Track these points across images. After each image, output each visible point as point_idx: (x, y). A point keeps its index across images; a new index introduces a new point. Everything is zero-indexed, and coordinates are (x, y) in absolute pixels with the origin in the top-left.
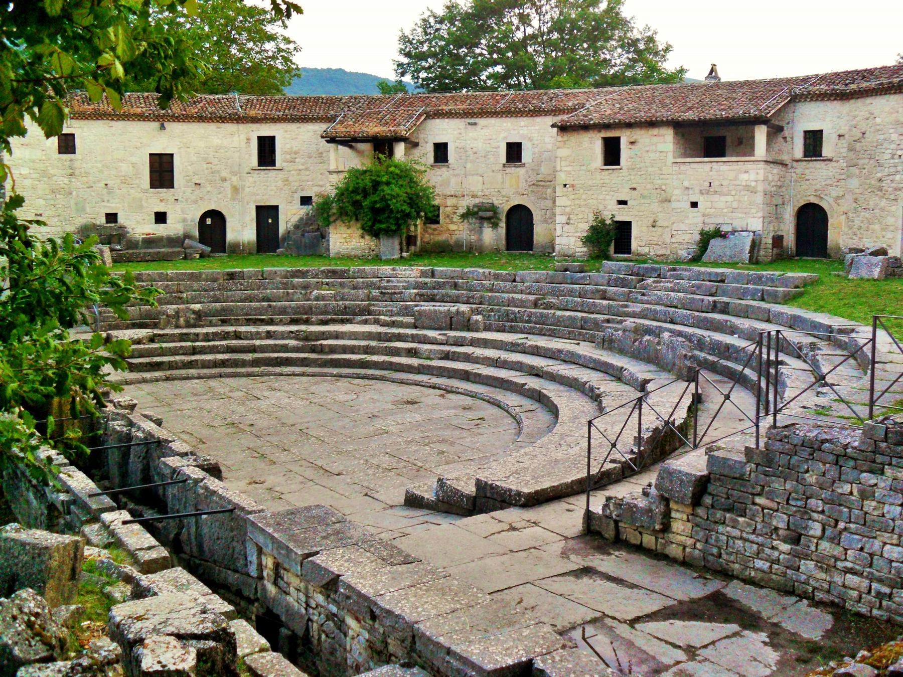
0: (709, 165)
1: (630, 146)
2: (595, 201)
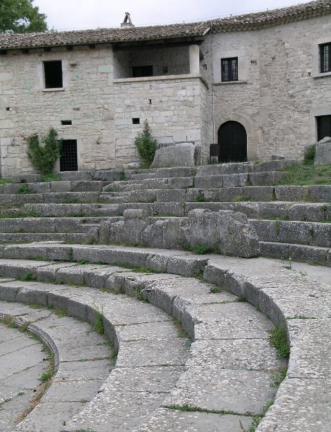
0: (147, 86)
1: (72, 69)
2: (39, 123)
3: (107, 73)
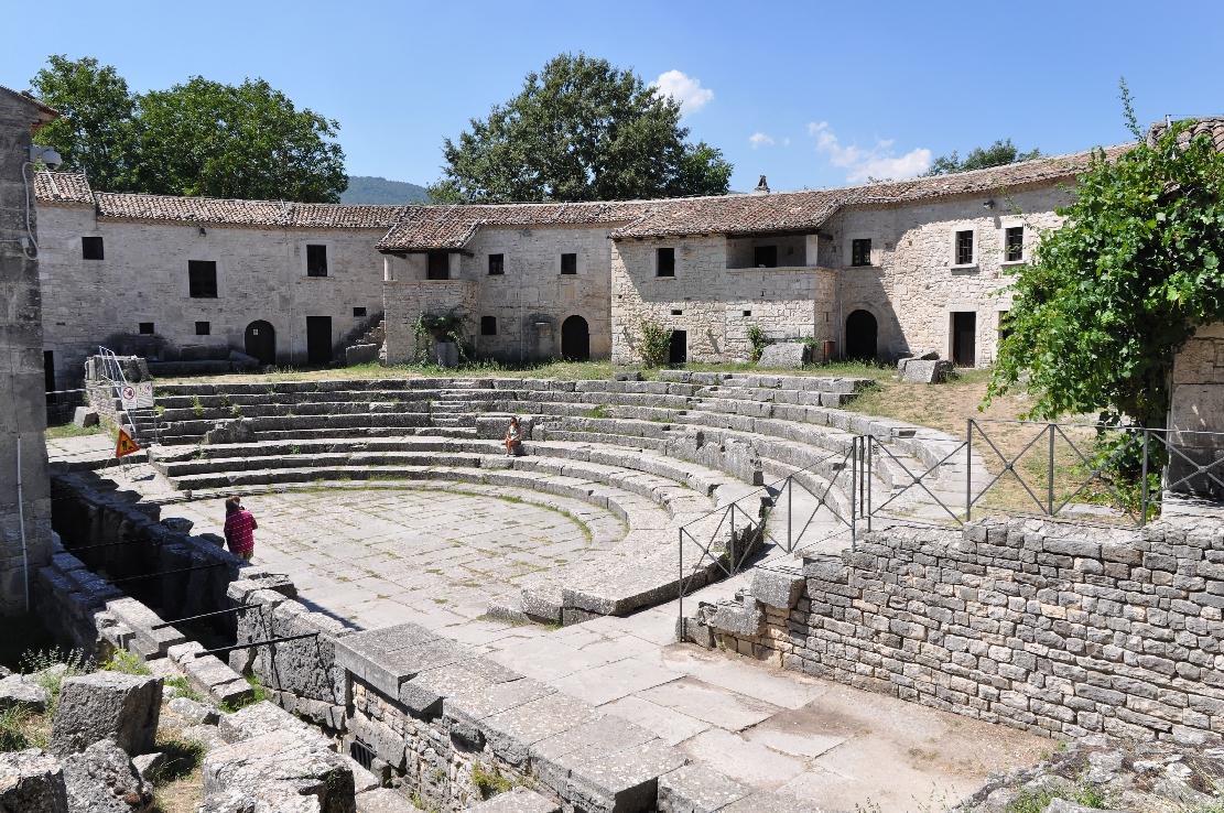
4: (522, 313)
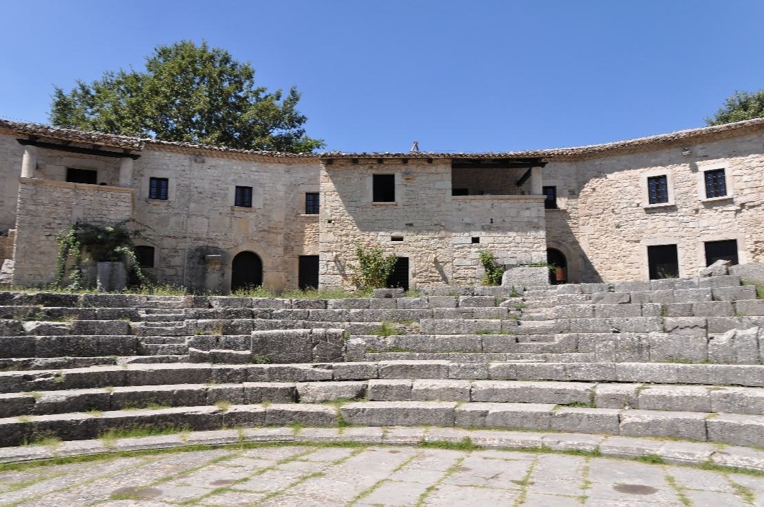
0: (488, 204)
3: (446, 190)
4: (186, 245)
